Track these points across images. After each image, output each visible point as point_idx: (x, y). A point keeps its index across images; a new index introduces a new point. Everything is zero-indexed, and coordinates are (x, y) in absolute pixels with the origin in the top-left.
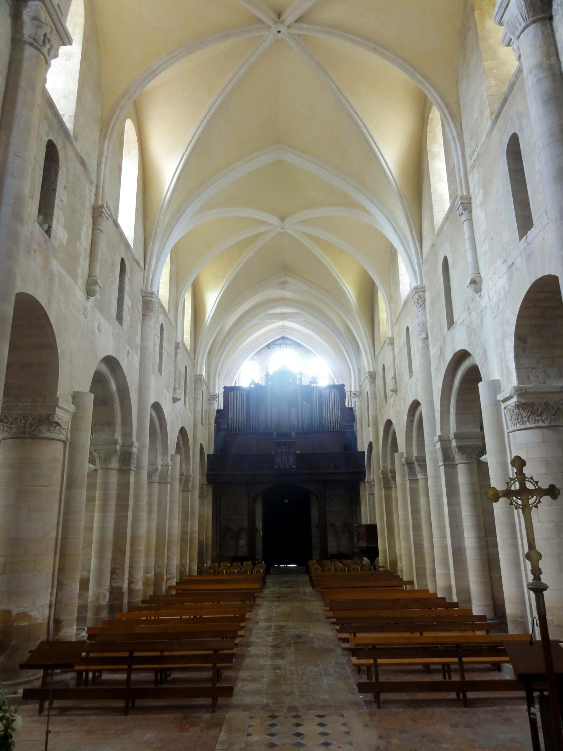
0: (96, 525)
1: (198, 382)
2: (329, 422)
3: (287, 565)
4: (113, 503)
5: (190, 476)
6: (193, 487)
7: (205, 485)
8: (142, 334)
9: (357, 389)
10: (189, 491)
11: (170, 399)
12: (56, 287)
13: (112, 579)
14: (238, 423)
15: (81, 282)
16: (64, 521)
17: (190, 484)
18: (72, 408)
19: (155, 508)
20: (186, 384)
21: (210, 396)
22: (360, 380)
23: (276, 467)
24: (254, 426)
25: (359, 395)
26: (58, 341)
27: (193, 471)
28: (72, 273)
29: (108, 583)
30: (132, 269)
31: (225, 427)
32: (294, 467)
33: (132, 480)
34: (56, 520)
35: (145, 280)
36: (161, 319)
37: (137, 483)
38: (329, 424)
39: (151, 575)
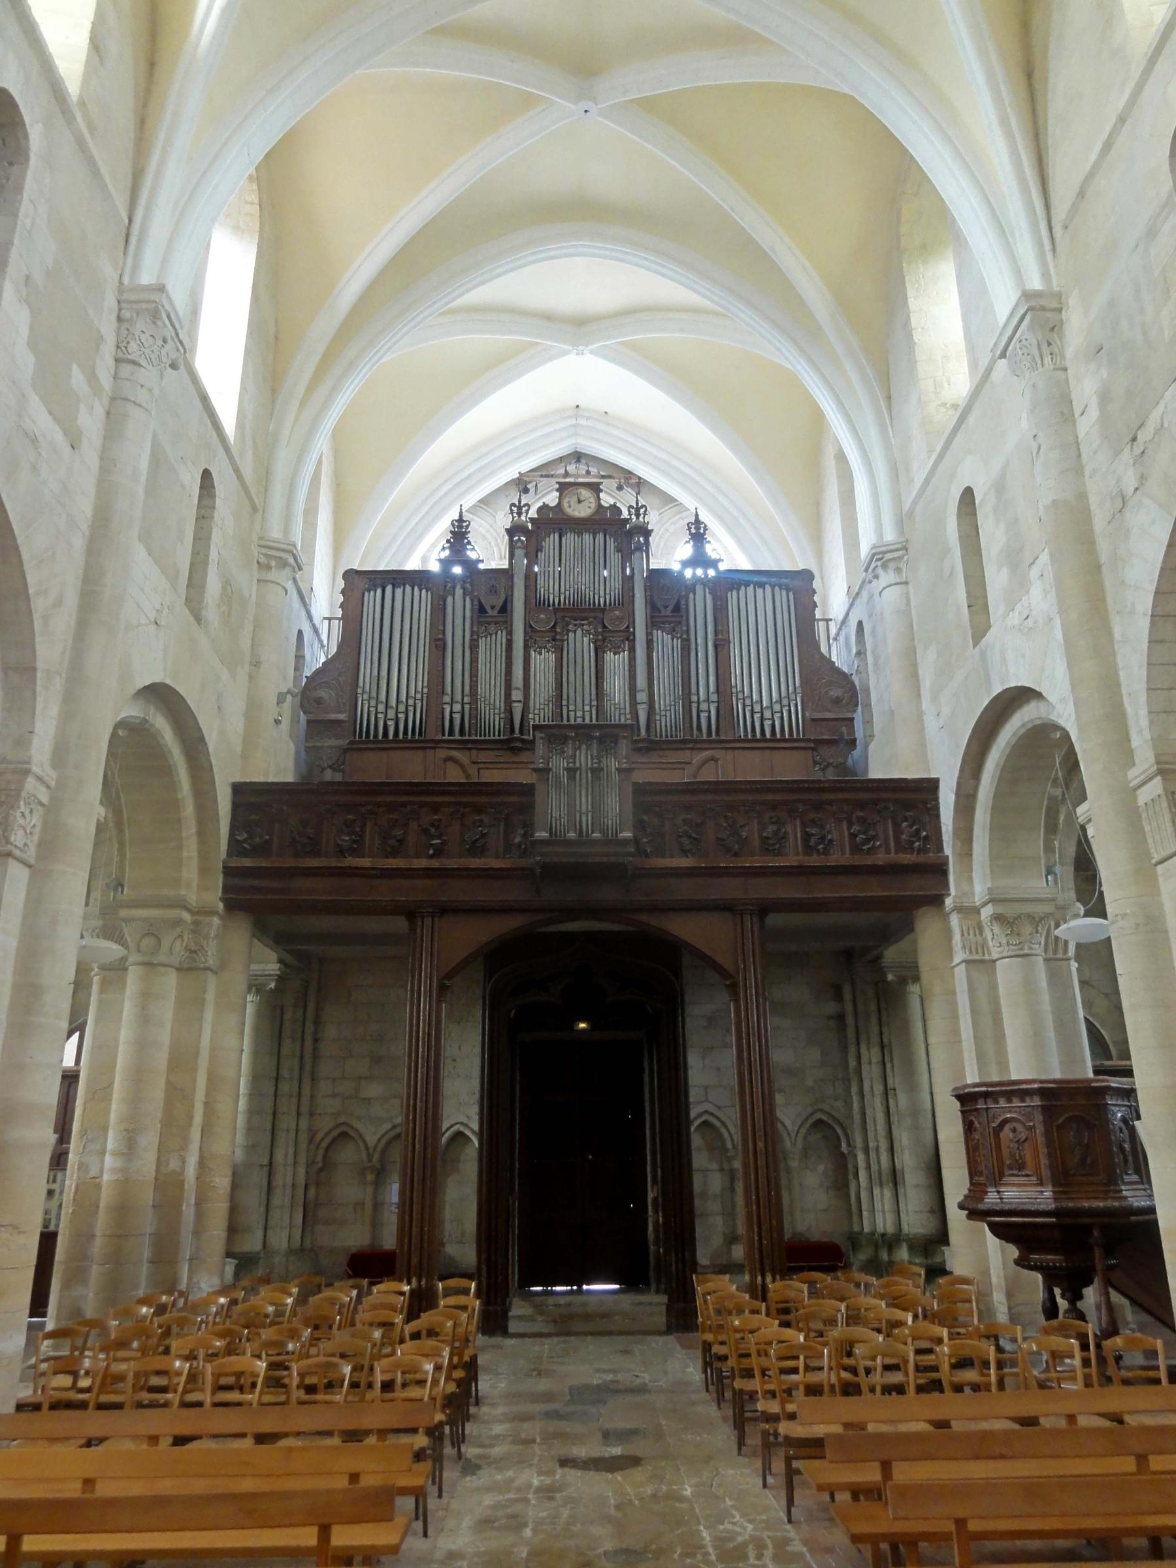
1: (140, 325)
2: (757, 708)
3: (580, 1286)
5: (27, 772)
7: (212, 913)
9: (890, 536)
10: (9, 854)
14: (393, 703)
21: (264, 551)
22: (897, 498)
23: (542, 834)
24: (457, 717)
25: (900, 558)
27: (59, 757)
31: (342, 717)
32: (627, 834)
38: (757, 716)
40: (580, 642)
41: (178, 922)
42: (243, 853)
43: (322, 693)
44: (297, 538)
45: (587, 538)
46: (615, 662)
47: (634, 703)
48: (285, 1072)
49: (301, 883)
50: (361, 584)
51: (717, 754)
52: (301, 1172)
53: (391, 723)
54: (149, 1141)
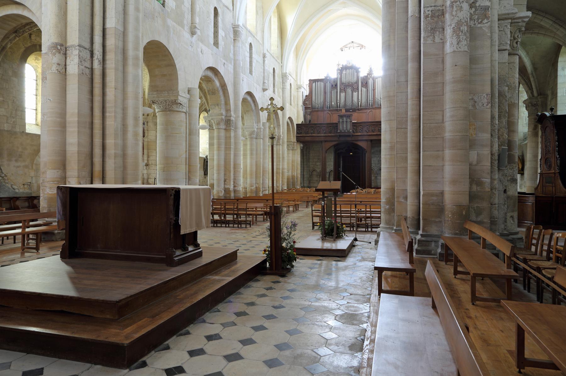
0: (215, 157)
4: (223, 146)
6: (283, 143)
8: (234, 51)
11: (260, 88)
12: (172, 33)
13: (225, 184)
15: (187, 28)
16: (189, 150)
17: (281, 141)
18: (188, 96)
19: (254, 152)
20: (275, 79)
26: (176, 62)
28: (181, 24)
29: (223, 186)
30: (223, 12)
31: (310, 106)
33: (232, 134)
34: (185, 149)
35: (234, 17)
36: (250, 40)
37: (236, 137)
39: (254, 188)
40: (349, 91)
41: (291, 144)
42: (298, 134)
43: (307, 102)
44: (302, 84)
45: (351, 70)
46: (355, 94)
47: (358, 102)
48: (305, 161)
49: (306, 138)
50: (312, 82)
51: (372, 110)
52: (308, 175)
53: (318, 107)
54: (290, 171)
